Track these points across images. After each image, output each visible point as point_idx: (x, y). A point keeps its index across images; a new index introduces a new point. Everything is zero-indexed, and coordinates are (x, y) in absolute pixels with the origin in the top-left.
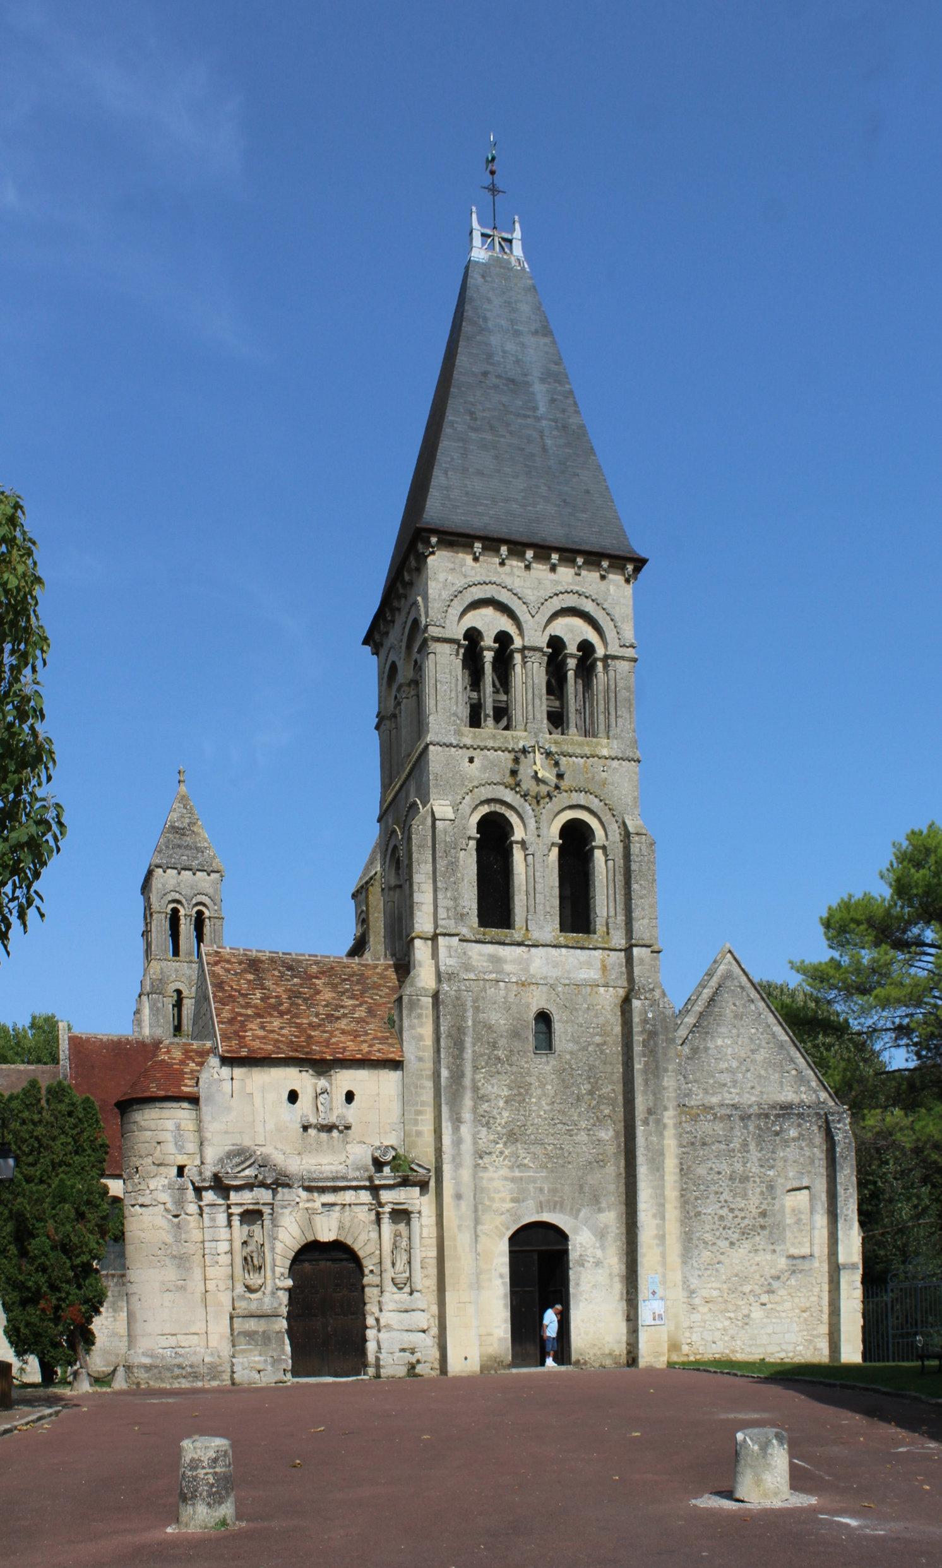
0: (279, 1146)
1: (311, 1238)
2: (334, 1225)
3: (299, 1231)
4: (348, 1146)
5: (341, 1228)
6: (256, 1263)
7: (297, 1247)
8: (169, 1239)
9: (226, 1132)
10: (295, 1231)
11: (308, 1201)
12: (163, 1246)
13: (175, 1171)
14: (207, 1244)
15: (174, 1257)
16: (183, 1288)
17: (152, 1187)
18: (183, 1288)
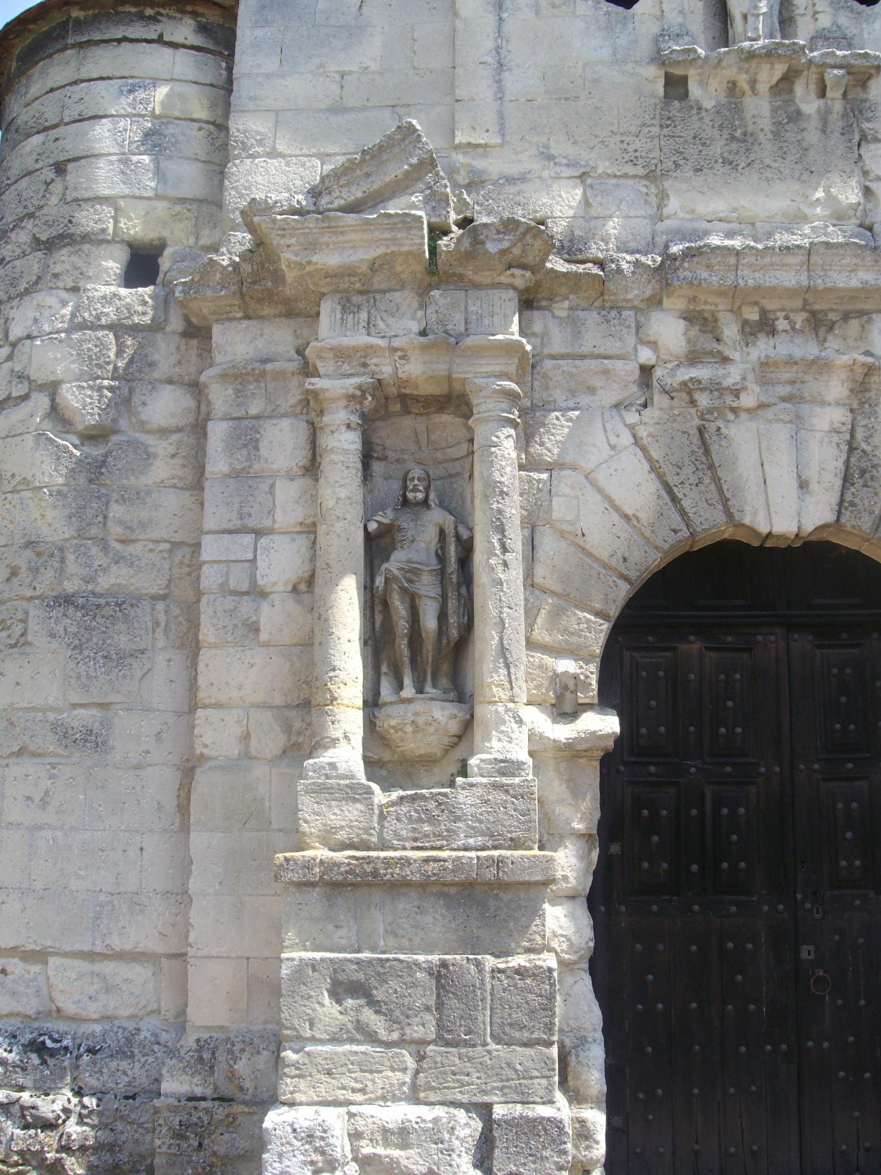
0: (561, 147)
1: (709, 523)
2: (826, 460)
3: (652, 486)
4: (869, 152)
5: (856, 471)
6: (430, 623)
7: (647, 560)
8: (53, 524)
9: (337, 109)
10: (633, 486)
11: (693, 358)
12: (23, 559)
13: (113, 264)
14: (212, 549)
15: (66, 600)
16: (91, 741)
17: (16, 332)
18: (91, 741)
